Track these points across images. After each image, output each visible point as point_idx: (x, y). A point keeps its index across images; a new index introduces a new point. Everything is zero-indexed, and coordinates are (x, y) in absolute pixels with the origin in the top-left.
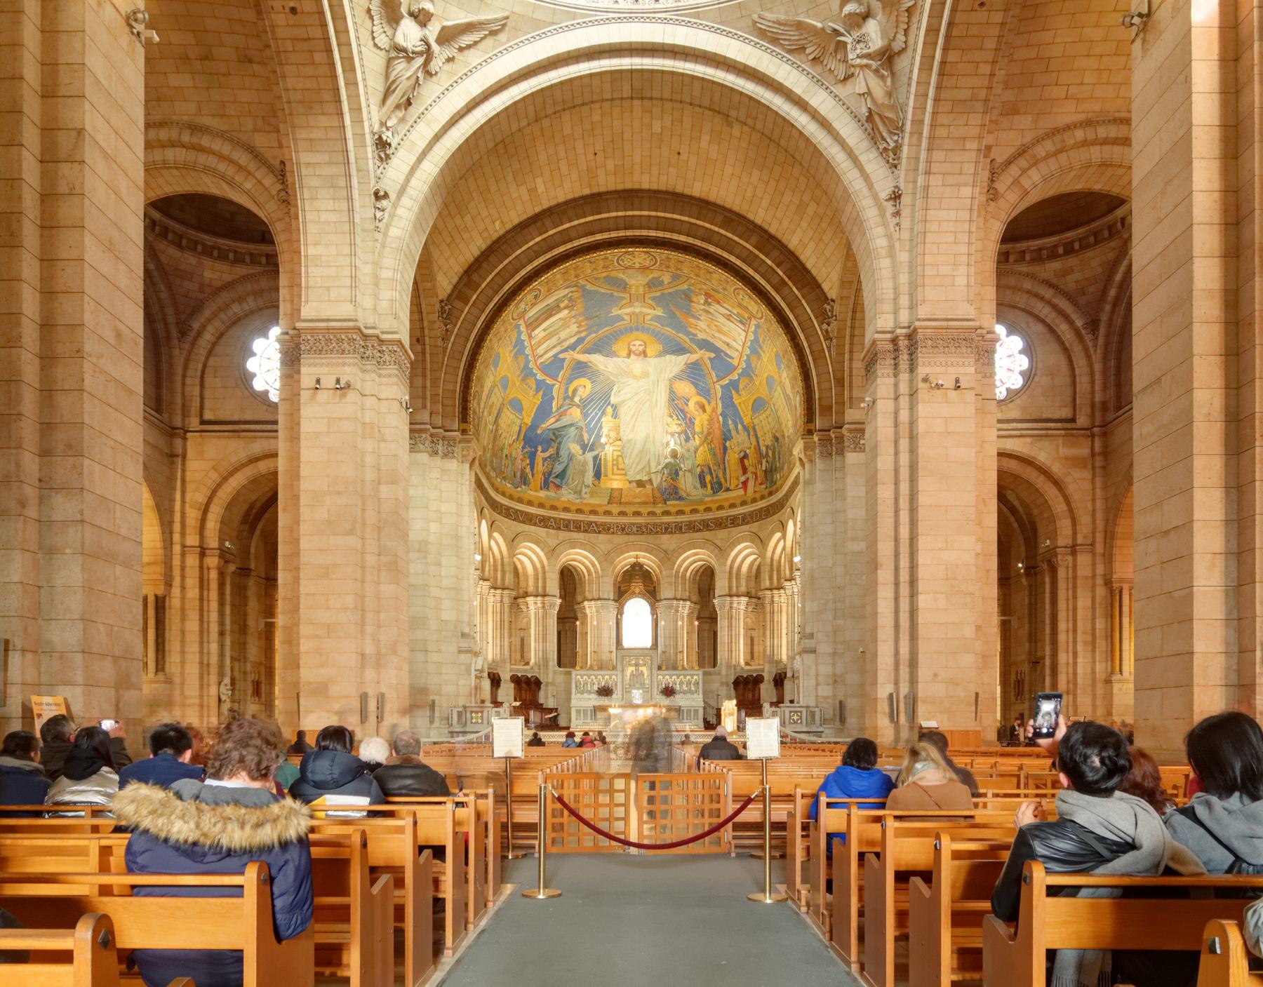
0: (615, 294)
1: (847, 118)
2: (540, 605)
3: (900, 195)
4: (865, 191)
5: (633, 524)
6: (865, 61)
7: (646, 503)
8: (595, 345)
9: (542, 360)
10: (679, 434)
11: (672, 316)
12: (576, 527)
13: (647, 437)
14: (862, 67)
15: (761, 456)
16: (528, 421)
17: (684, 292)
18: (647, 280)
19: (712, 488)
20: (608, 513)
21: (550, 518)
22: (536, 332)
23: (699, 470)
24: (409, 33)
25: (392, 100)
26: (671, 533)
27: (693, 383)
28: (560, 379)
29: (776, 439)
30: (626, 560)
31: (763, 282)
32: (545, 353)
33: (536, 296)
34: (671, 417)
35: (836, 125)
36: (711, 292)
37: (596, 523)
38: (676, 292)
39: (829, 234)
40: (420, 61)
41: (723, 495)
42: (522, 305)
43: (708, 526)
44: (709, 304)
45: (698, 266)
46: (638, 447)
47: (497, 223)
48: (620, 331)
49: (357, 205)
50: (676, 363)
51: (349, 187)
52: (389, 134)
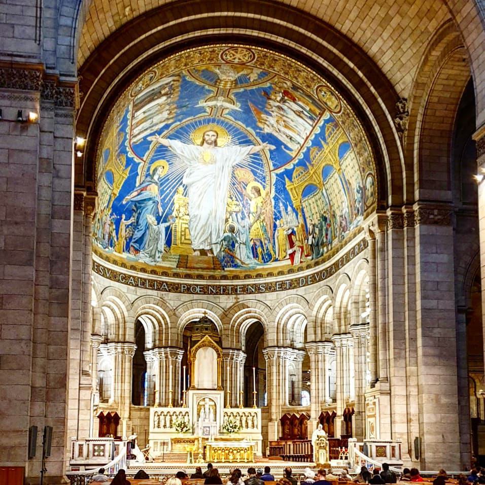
0: (207, 87)
2: (120, 350)
5: (197, 285)
8: (177, 132)
9: (134, 140)
10: (237, 213)
11: (247, 111)
13: (210, 214)
16: (117, 192)
19: (263, 258)
22: (138, 113)
23: (252, 243)
26: (229, 294)
27: (252, 171)
28: (145, 158)
29: (325, 219)
31: (345, 81)
32: (139, 134)
33: (151, 79)
34: (231, 198)
36: (290, 90)
38: (258, 90)
39: (409, 43)
41: (272, 265)
43: (259, 289)
44: (285, 102)
45: (289, 65)
46: (202, 222)
47: (127, 9)
48: (200, 122)
50: (241, 153)
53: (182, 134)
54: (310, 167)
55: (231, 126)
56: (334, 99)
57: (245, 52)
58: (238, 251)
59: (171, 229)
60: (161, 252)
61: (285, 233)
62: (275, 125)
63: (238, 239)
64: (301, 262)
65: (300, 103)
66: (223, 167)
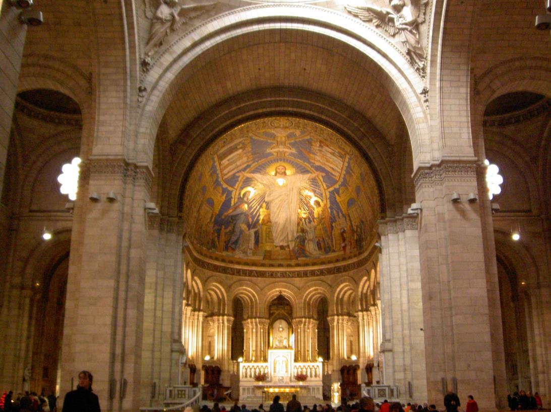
0: (269, 141)
3: (427, 92)
4: (410, 90)
5: (278, 272)
6: (404, 26)
7: (286, 259)
8: (257, 168)
9: (226, 177)
10: (305, 219)
11: (300, 152)
12: (243, 273)
13: (287, 220)
14: (403, 29)
15: (353, 232)
16: (217, 211)
17: (307, 140)
18: (287, 134)
20: (263, 265)
21: (228, 268)
24: (164, 11)
25: (152, 43)
26: (301, 277)
28: (236, 187)
29: (362, 222)
30: (274, 292)
33: (224, 142)
34: (300, 209)
35: (390, 56)
36: (323, 140)
37: (256, 271)
40: (169, 24)
42: (216, 147)
44: (322, 147)
45: (316, 127)
46: (281, 226)
49: (129, 94)
51: (125, 85)
52: (149, 59)
53: (261, 170)
54: (349, 187)
55: (293, 162)
56: (347, 147)
57: (285, 121)
58: (307, 246)
59: (259, 234)
60: (251, 249)
61: (339, 232)
62: (321, 161)
63: (307, 237)
64: (350, 252)
65: (331, 148)
66: (292, 189)
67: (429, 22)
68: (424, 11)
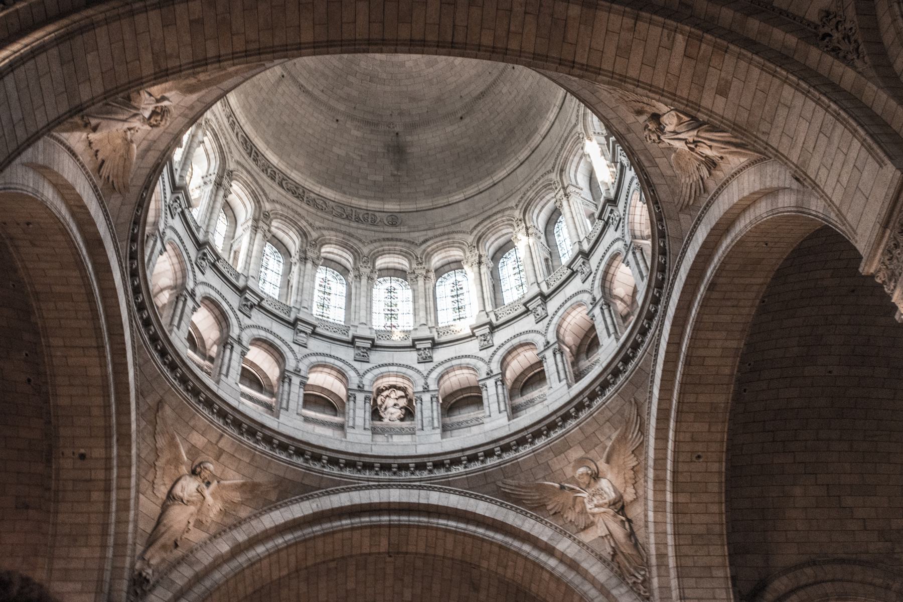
1: (592, 560)
6: (602, 510)
35: (585, 565)
52: (150, 571)
67: (646, 498)
68: (634, 482)
